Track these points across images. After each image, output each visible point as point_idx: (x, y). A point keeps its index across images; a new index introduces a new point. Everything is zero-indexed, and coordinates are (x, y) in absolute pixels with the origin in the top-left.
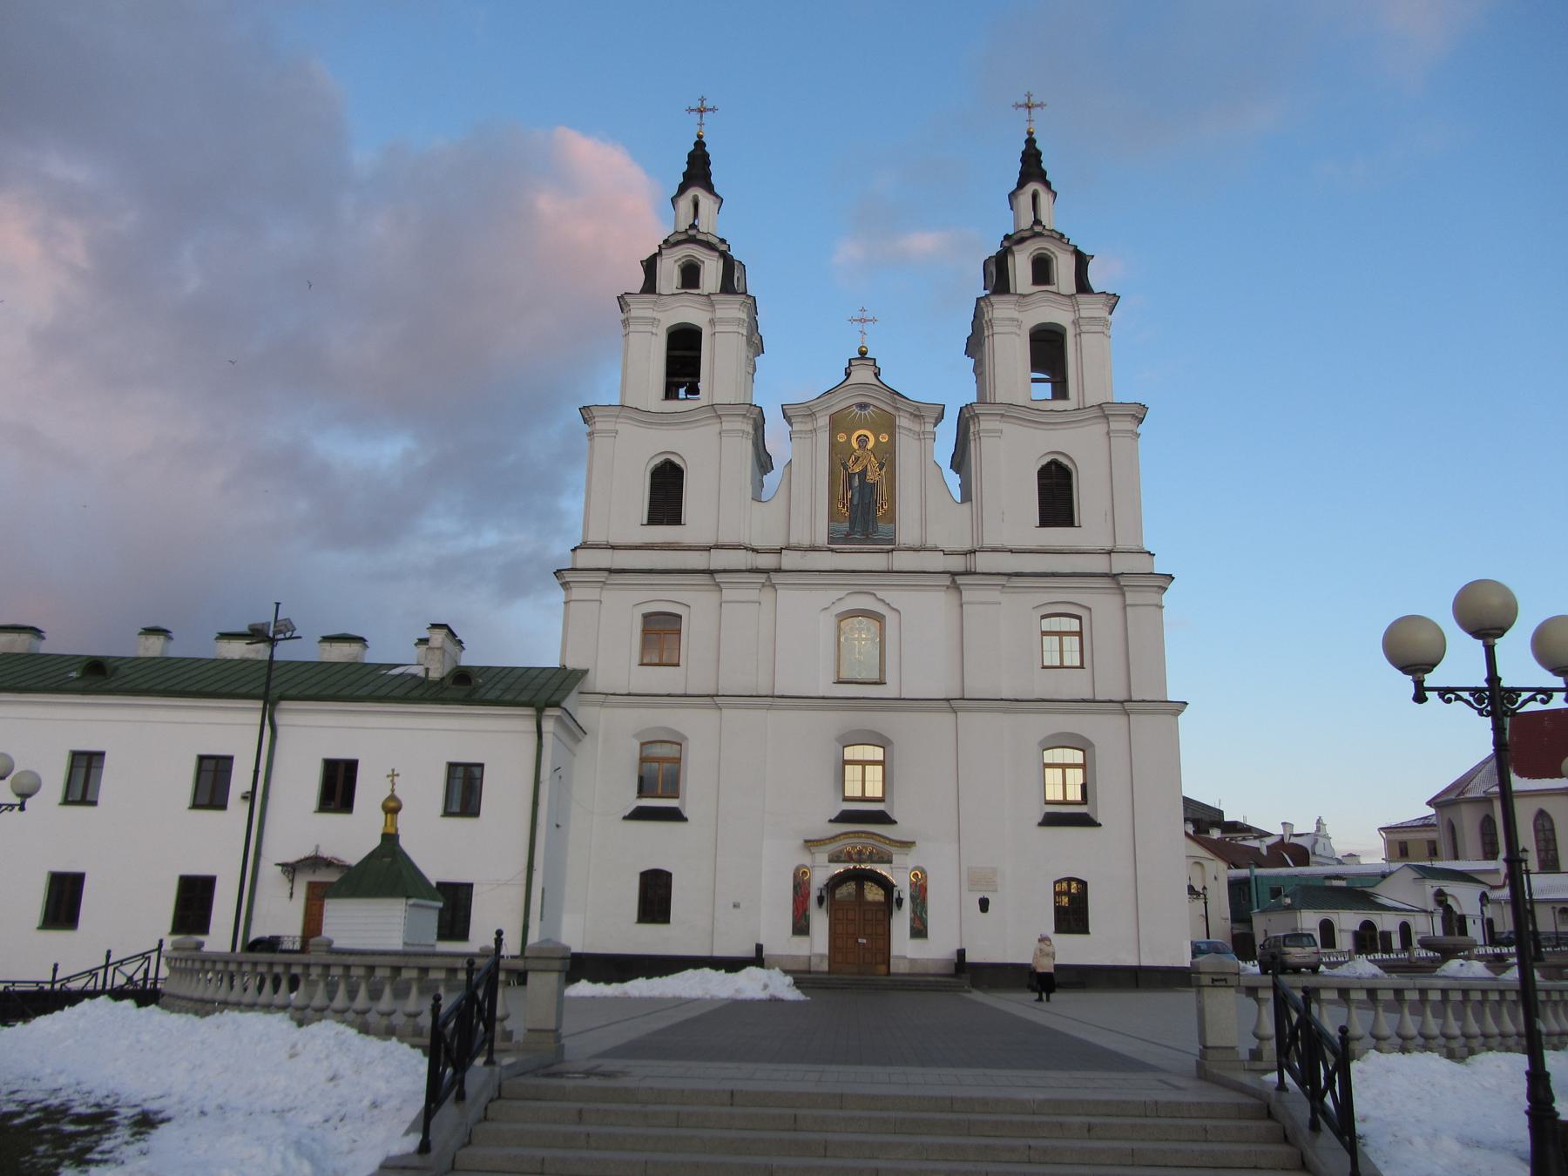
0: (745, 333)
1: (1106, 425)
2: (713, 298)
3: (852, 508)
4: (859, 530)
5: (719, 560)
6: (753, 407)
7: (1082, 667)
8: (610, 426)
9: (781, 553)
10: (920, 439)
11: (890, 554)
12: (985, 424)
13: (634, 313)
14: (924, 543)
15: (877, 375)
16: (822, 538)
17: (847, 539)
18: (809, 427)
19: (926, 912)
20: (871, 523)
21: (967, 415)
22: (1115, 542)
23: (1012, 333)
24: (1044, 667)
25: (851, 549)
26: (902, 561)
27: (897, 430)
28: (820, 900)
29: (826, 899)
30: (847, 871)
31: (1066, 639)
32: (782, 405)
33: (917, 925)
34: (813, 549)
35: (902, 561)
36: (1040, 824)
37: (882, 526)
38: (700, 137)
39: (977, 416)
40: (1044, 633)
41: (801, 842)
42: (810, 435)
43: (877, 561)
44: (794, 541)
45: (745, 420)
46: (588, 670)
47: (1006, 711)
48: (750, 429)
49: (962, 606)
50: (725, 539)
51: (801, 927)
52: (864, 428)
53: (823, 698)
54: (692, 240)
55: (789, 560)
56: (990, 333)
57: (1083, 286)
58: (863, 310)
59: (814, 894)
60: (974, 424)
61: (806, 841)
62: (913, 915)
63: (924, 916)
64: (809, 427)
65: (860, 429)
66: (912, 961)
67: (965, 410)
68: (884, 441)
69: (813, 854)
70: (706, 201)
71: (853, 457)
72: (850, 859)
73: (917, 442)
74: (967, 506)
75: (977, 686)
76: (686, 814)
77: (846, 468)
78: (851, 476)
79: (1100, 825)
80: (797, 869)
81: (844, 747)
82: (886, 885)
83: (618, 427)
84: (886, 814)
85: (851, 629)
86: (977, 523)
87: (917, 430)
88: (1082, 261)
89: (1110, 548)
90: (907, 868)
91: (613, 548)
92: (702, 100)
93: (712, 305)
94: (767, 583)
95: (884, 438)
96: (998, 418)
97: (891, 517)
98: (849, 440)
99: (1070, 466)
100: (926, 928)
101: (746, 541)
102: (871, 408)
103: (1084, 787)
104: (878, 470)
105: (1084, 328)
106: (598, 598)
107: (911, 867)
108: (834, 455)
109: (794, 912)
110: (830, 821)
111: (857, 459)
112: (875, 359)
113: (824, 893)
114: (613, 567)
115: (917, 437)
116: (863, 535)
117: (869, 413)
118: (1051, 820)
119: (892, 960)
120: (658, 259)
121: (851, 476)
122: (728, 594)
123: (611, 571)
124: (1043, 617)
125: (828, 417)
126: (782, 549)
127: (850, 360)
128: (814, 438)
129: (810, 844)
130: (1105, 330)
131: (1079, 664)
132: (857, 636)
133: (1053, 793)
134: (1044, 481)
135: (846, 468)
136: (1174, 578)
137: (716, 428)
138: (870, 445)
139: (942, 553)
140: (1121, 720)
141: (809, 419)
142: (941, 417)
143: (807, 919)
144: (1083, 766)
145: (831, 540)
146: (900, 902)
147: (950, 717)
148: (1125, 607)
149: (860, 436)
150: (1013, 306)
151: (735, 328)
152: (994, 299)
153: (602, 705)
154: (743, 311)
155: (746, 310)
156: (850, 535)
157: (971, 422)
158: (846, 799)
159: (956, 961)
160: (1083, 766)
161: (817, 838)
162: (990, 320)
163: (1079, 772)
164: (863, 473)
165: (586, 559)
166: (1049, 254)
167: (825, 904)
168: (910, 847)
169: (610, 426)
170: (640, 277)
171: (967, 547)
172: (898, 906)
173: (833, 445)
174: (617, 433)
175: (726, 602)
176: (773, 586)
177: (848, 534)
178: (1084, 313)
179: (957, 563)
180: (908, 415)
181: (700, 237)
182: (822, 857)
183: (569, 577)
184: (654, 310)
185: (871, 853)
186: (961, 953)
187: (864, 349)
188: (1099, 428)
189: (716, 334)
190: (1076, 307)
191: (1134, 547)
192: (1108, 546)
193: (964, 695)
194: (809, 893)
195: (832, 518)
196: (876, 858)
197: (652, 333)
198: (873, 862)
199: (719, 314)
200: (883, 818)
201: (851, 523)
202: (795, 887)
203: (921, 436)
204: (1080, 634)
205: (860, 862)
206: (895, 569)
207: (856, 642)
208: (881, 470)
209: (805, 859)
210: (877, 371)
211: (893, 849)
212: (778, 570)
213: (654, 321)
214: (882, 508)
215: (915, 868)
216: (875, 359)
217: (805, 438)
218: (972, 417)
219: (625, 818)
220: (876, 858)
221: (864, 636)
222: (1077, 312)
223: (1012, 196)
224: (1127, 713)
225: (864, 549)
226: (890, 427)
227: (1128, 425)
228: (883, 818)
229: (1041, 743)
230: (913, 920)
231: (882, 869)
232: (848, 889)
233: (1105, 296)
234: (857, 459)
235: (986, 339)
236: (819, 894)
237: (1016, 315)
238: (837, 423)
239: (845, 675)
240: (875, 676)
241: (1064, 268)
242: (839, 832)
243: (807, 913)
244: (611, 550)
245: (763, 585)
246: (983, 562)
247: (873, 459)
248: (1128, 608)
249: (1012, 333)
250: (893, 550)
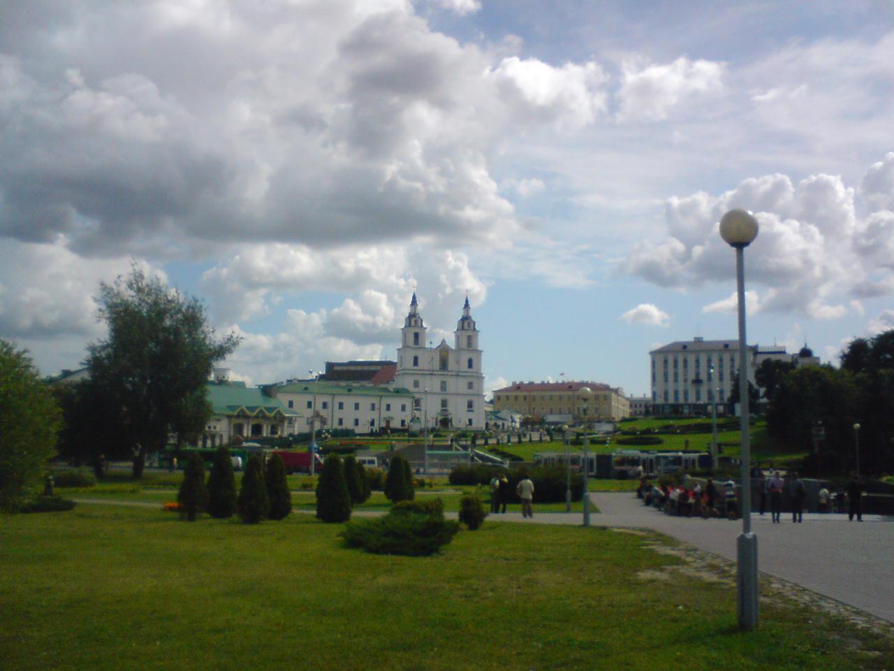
5: (424, 372)
26: (449, 373)
35: (449, 373)
51: (436, 424)
55: (434, 373)
57: (474, 329)
88: (474, 323)
129: (438, 414)
173: (440, 355)
212: (432, 374)
238: (441, 351)
241: (472, 324)
246: (460, 374)
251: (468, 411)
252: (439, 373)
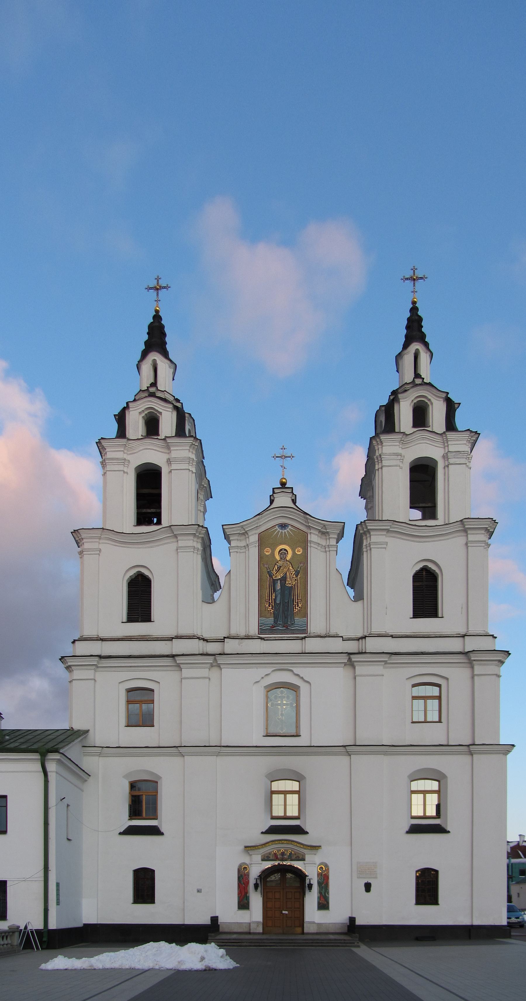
0: (194, 471)
1: (464, 538)
2: (169, 440)
3: (276, 606)
4: (281, 623)
5: (179, 647)
6: (201, 528)
7: (440, 721)
8: (95, 546)
9: (224, 641)
10: (326, 552)
11: (304, 640)
12: (375, 538)
13: (109, 455)
14: (328, 632)
15: (294, 501)
16: (254, 630)
17: (272, 630)
18: (243, 544)
19: (328, 893)
20: (289, 617)
21: (361, 532)
22: (468, 629)
23: (396, 466)
24: (413, 722)
25: (275, 637)
27: (309, 544)
28: (256, 886)
29: (260, 885)
30: (274, 866)
31: (429, 702)
32: (223, 525)
33: (322, 901)
34: (248, 638)
35: (312, 645)
36: (408, 832)
38: (157, 311)
39: (369, 531)
40: (414, 698)
41: (242, 847)
42: (244, 550)
43: (294, 646)
44: (233, 632)
45: (195, 539)
46: (89, 730)
47: (385, 753)
48: (199, 546)
49: (355, 678)
50: (182, 632)
51: (244, 904)
52: (284, 544)
53: (256, 747)
54: (152, 395)
55: (231, 646)
56: (380, 466)
57: (451, 426)
58: (283, 448)
59: (252, 882)
60: (367, 539)
61: (246, 847)
62: (319, 894)
63: (327, 895)
64: (243, 544)
65: (281, 544)
66: (319, 924)
67: (360, 528)
68: (299, 553)
69: (251, 855)
70: (163, 366)
71: (276, 566)
72: (276, 859)
73: (325, 554)
74: (360, 603)
75: (364, 737)
76: (162, 830)
77: (271, 576)
78: (274, 582)
79: (449, 832)
80: (240, 866)
81: (272, 781)
82: (301, 876)
83: (101, 546)
84: (301, 827)
85: (276, 697)
86: (367, 617)
87: (324, 544)
89: (464, 633)
90: (315, 864)
91: (102, 640)
92: (158, 279)
93: (168, 447)
94: (214, 664)
95: (299, 551)
96: (385, 533)
97: (305, 614)
98: (273, 554)
99: (437, 571)
100: (328, 903)
101: (199, 633)
102: (290, 527)
103: (438, 807)
104: (294, 576)
105: (451, 461)
106: (92, 677)
107: (318, 863)
108: (262, 565)
109: (238, 894)
110: (262, 833)
111: (279, 568)
112: (292, 488)
113: (259, 882)
114: (103, 655)
115: (324, 550)
116: (284, 626)
117: (288, 531)
118: (415, 829)
119: (305, 925)
120: (127, 412)
121: (274, 582)
122: (186, 672)
123: (100, 657)
124: (414, 686)
125: (257, 536)
126: (225, 638)
127: (273, 489)
128: (247, 552)
130: (467, 462)
131: (437, 720)
132: (279, 702)
133: (417, 811)
134: (418, 584)
135: (271, 576)
136: (510, 654)
137: (173, 546)
138: (289, 557)
139: (342, 638)
140: (466, 759)
141: (243, 537)
142: (341, 535)
143: (247, 898)
144: (438, 792)
145: (261, 631)
146: (310, 886)
147: (346, 759)
148: (473, 677)
149: (281, 550)
150: (398, 444)
151: (185, 466)
152: (383, 437)
153: (100, 755)
154: (192, 452)
155: (194, 452)
156: (275, 627)
157: (364, 537)
158: (273, 818)
159: (348, 924)
160: (438, 792)
161: (253, 844)
162: (380, 455)
163: (435, 796)
164: (284, 579)
165: (82, 648)
166: (426, 401)
167: (259, 889)
168: (317, 850)
169: (95, 546)
170: (114, 427)
171: (360, 635)
172: (309, 889)
174: (100, 550)
175: (185, 678)
176: (219, 666)
178: (452, 448)
179: (352, 647)
180: (317, 533)
181: (159, 394)
182: (257, 857)
183: (71, 662)
184: (124, 453)
185: (291, 854)
186: (352, 920)
187: (284, 480)
188: (460, 540)
189: (172, 471)
190: (445, 444)
191: (482, 633)
192: (463, 631)
193: (355, 742)
194: (249, 881)
195: (261, 614)
196: (294, 858)
197: (124, 472)
198: (292, 860)
199: (174, 454)
200: (299, 830)
201: (274, 617)
202: (239, 878)
203: (326, 549)
204: (439, 698)
205: (283, 860)
206: (307, 652)
207: (279, 707)
208: (297, 576)
209: (246, 859)
210: (294, 498)
211: (305, 851)
213: (125, 462)
214: (298, 606)
215: (322, 863)
216: (292, 488)
217: (240, 552)
218: (365, 533)
219: (120, 834)
220: (294, 858)
221: (285, 702)
222: (446, 448)
223: (399, 357)
224: (471, 754)
225: (284, 637)
226: (304, 543)
227: (482, 537)
228: (299, 830)
229: (409, 776)
230: (319, 898)
231: (298, 865)
232: (276, 877)
233: (468, 433)
234: (279, 568)
235: (377, 472)
236: (255, 882)
237: (400, 451)
239: (272, 731)
240: (293, 731)
242: (268, 840)
243: (248, 895)
244: (100, 641)
245: (212, 666)
247: (291, 568)
248: (476, 677)
249: (396, 466)
250: (305, 638)
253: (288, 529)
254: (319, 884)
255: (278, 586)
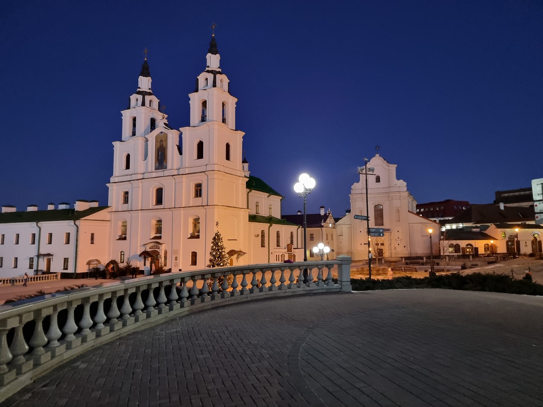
37: (165, 164)
55: (146, 176)
72: (153, 248)
145: (155, 169)
177: (158, 167)
195: (155, 164)
196: (157, 248)
201: (159, 164)
251: (192, 237)
252: (154, 175)
253: (163, 134)
254: (165, 257)
255: (160, 153)
